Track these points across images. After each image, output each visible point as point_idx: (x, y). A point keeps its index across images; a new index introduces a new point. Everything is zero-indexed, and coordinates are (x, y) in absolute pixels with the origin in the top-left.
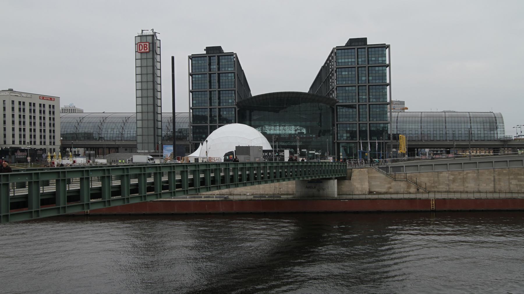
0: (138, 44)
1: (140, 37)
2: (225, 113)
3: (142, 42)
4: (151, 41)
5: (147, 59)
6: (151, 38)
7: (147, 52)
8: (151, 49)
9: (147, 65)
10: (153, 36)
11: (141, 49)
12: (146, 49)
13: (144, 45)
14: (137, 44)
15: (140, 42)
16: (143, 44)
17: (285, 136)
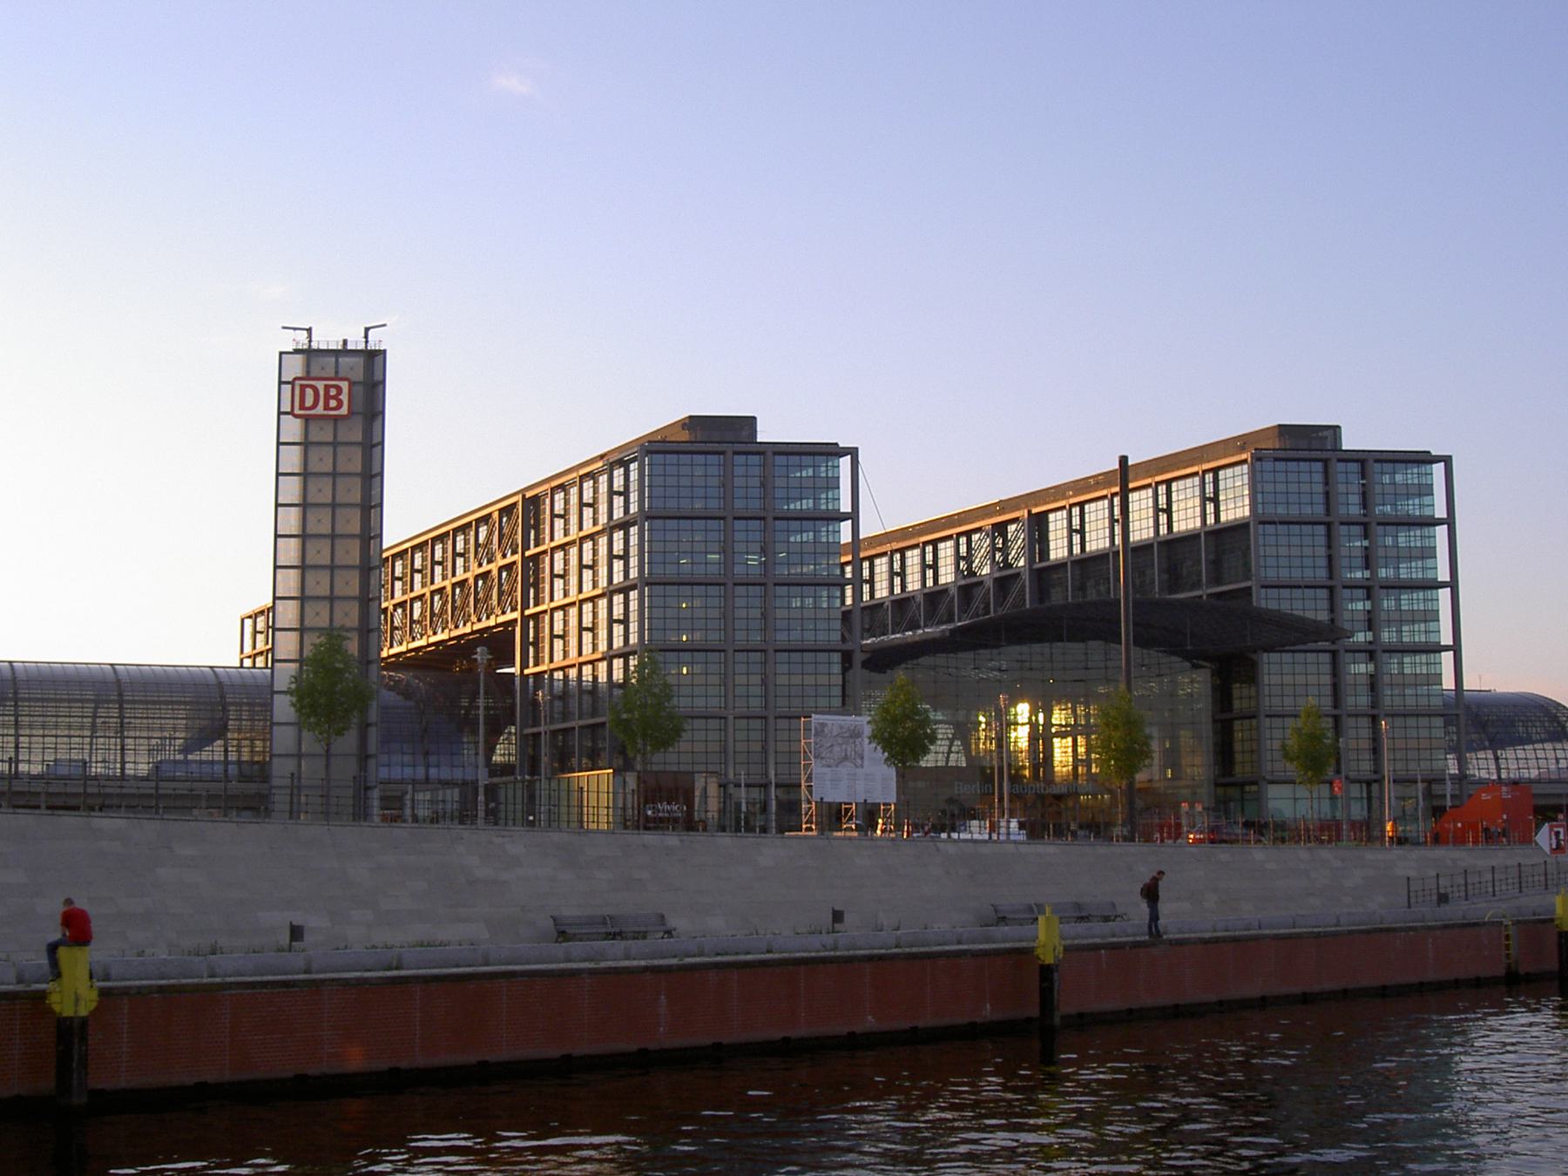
0: (298, 383)
1: (299, 357)
3: (313, 374)
4: (359, 375)
6: (359, 361)
7: (336, 419)
8: (359, 407)
10: (373, 359)
11: (309, 402)
12: (333, 403)
13: (327, 388)
14: (292, 383)
15: (299, 375)
16: (320, 385)
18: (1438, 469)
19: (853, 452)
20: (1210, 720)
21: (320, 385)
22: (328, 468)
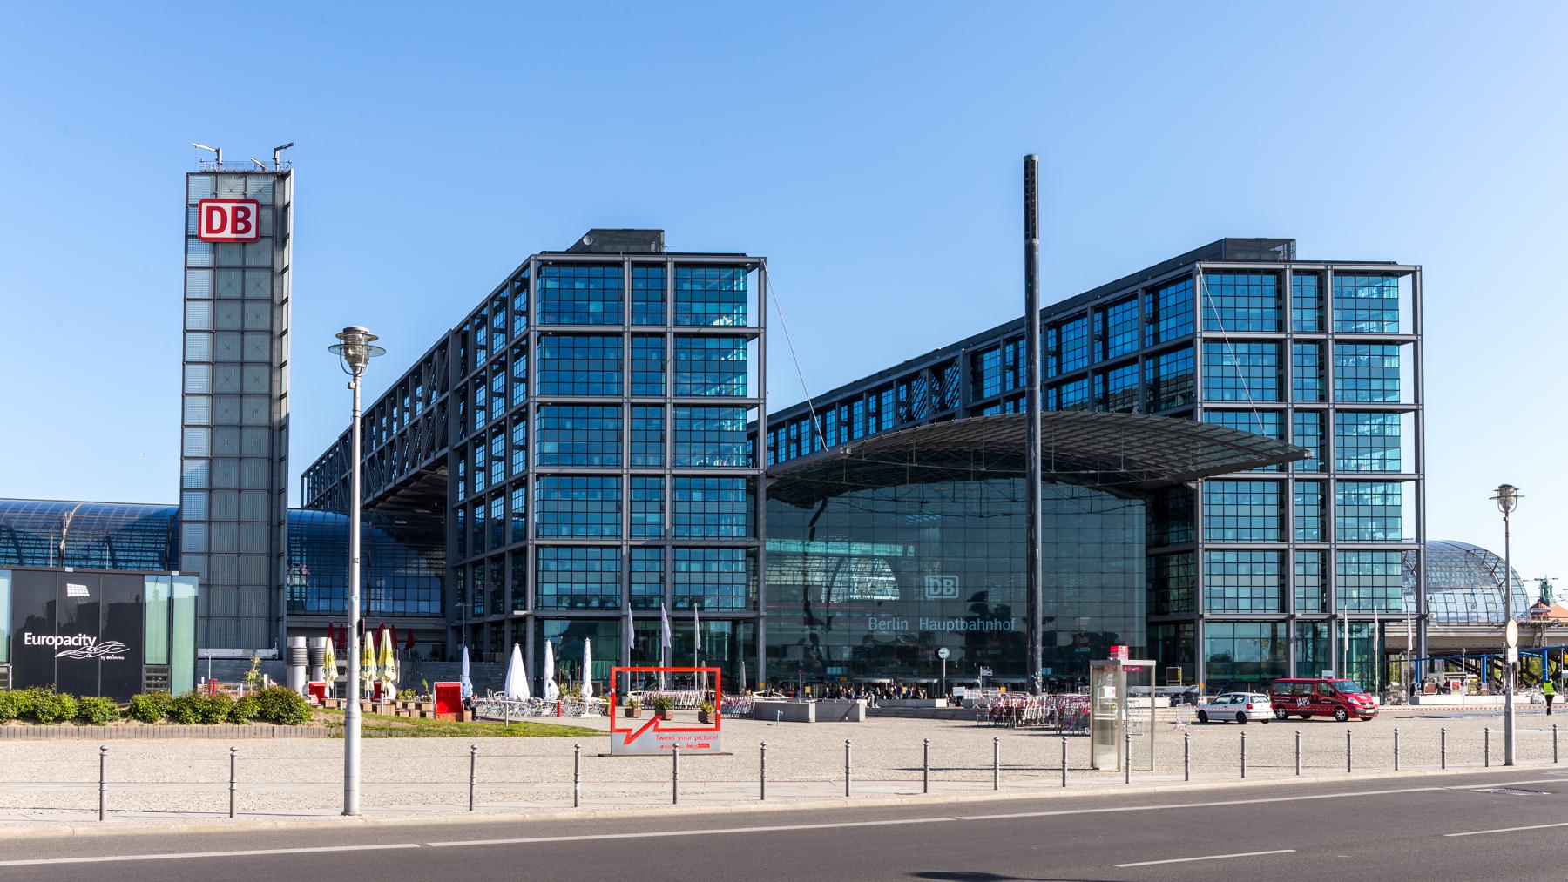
0: (205, 205)
1: (208, 178)
2: (697, 496)
5: (243, 269)
7: (244, 242)
8: (267, 229)
9: (243, 294)
11: (216, 224)
12: (241, 226)
13: (235, 210)
15: (208, 196)
16: (228, 207)
17: (942, 594)
18: (1405, 283)
19: (759, 265)
20: (1144, 556)
21: (228, 207)
22: (237, 293)
